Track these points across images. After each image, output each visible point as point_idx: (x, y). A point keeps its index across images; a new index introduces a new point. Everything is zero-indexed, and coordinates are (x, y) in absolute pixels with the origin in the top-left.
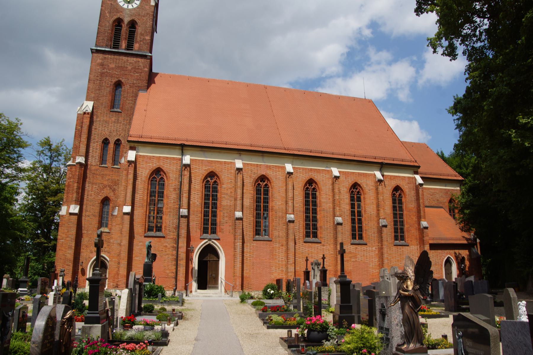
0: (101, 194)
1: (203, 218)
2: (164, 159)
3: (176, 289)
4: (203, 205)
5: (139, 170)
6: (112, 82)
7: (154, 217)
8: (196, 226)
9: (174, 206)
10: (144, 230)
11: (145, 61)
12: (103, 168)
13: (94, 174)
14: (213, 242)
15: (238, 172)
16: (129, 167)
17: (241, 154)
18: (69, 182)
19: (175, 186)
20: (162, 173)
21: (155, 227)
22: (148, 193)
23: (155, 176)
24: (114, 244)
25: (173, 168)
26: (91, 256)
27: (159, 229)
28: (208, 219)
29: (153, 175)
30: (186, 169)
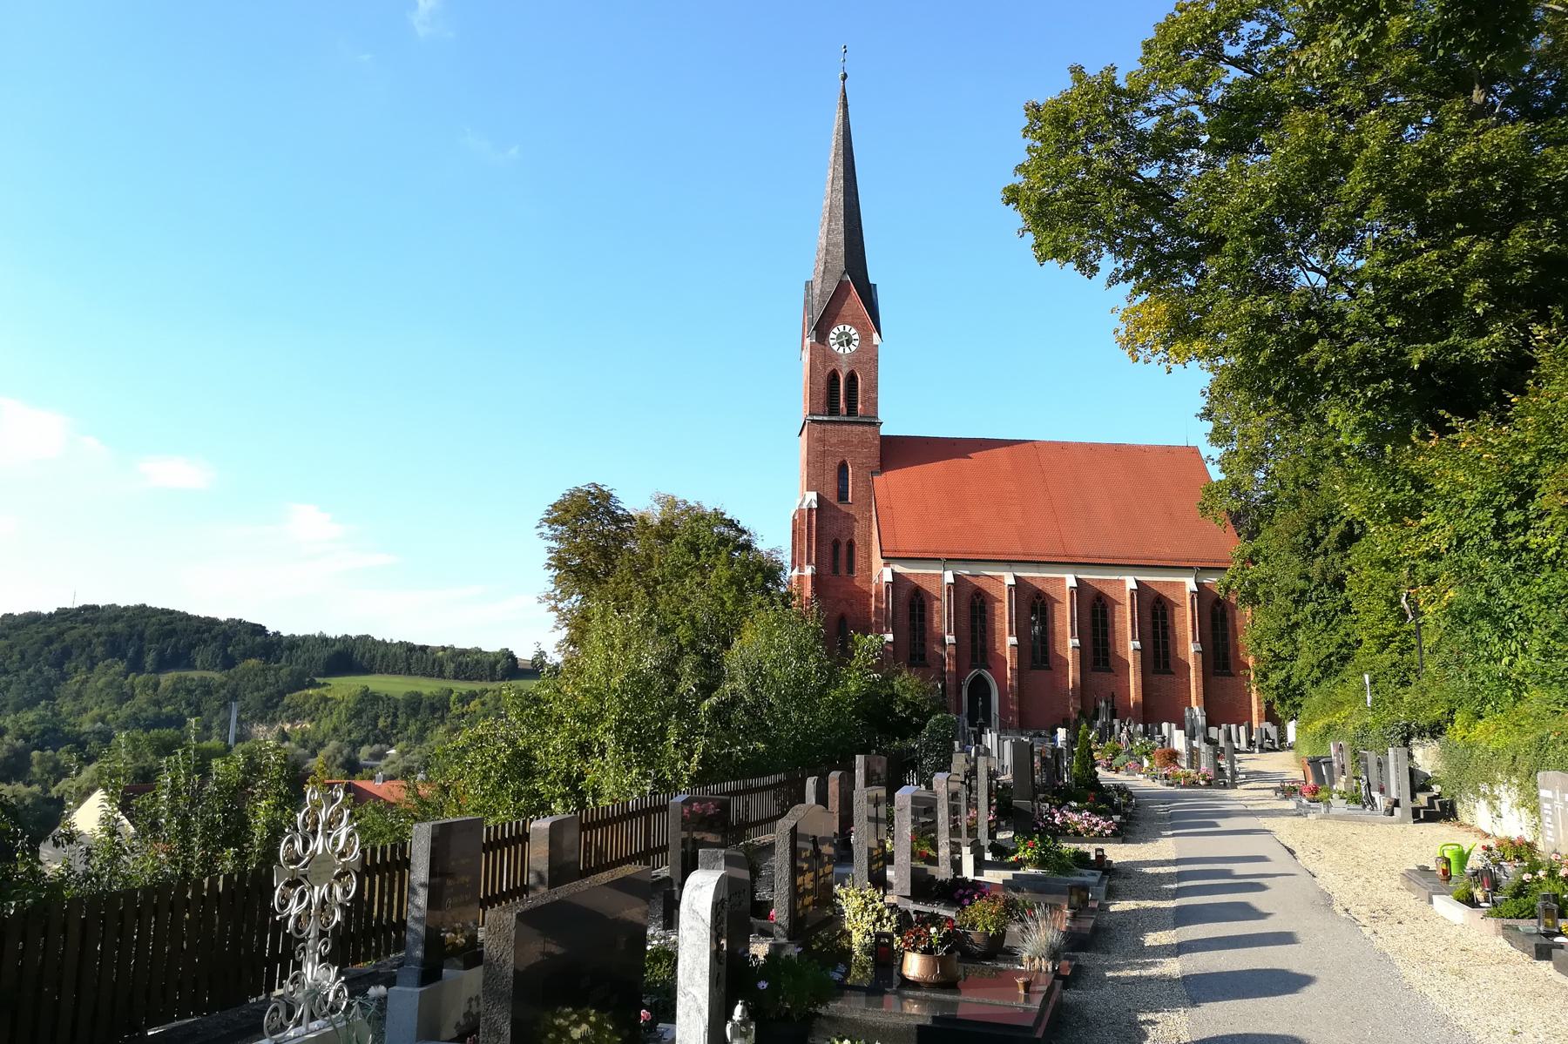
27: (923, 657)
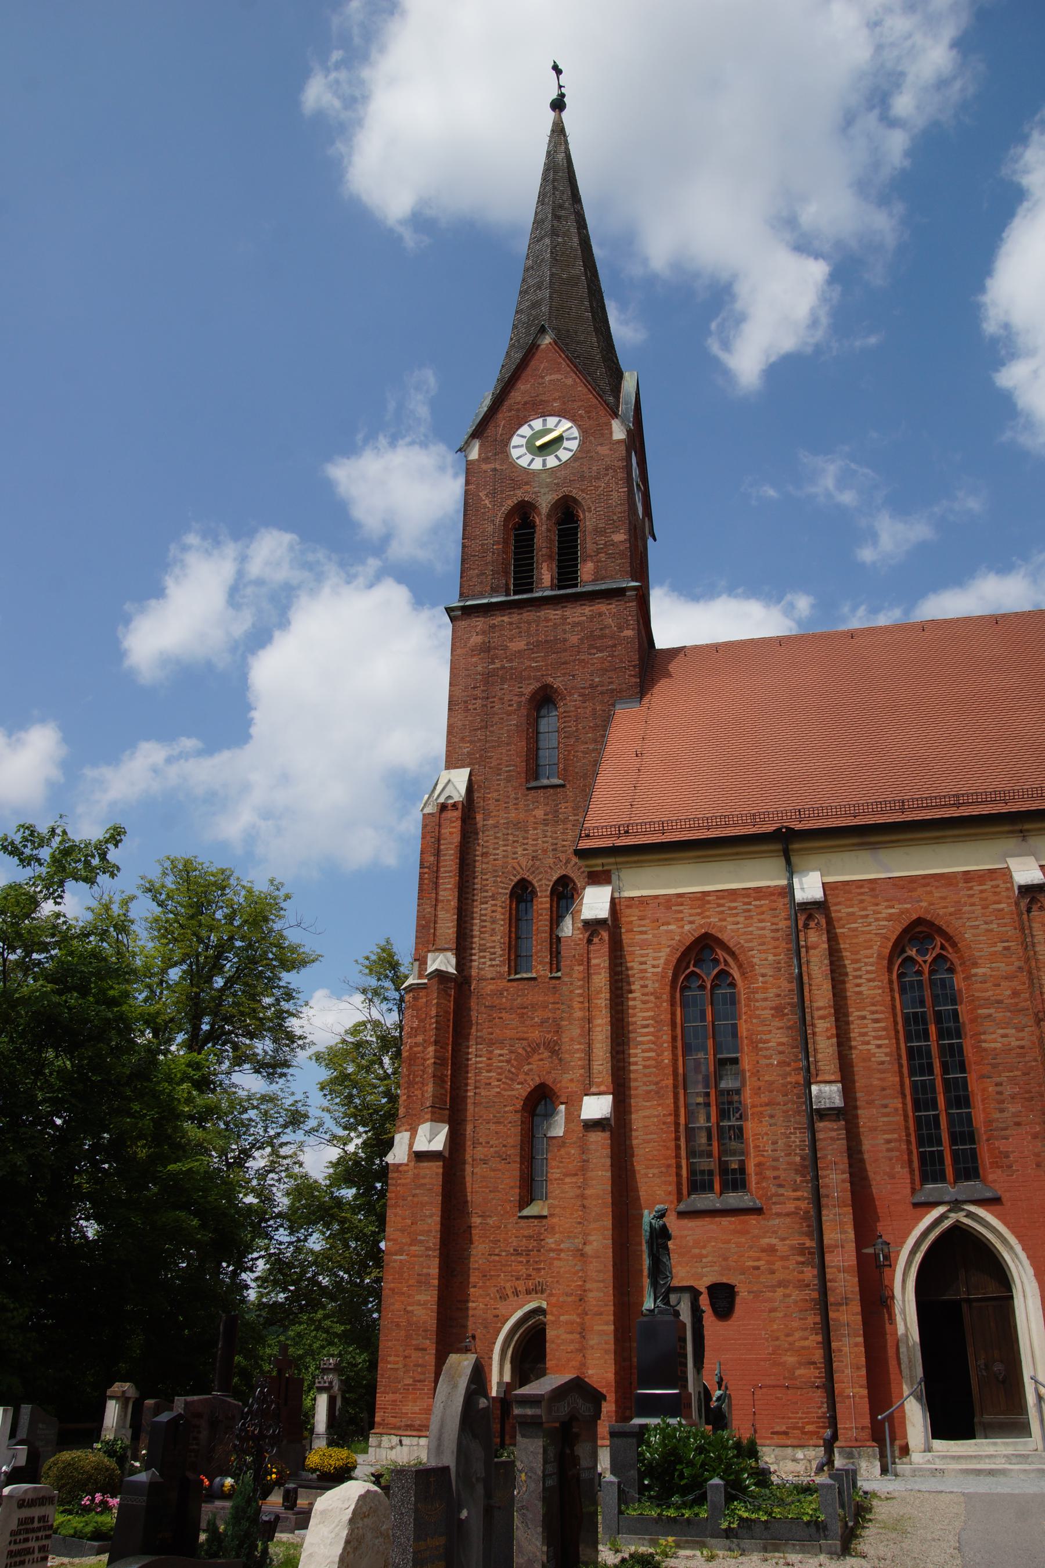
0: (521, 1077)
1: (910, 1114)
2: (723, 898)
3: (835, 1437)
4: (904, 1062)
5: (632, 953)
6: (521, 694)
7: (709, 1130)
8: (889, 1150)
9: (785, 1076)
10: (672, 1188)
11: (621, 608)
12: (521, 985)
13: (492, 1007)
14: (970, 1215)
15: (1031, 902)
16: (592, 948)
17: (1028, 831)
18: (411, 1047)
19: (779, 995)
20: (721, 954)
21: (717, 1171)
22: (674, 1038)
23: (695, 969)
24: (562, 1255)
25: (763, 929)
26: (504, 1312)
27: (736, 1180)
28: (936, 1118)
29: (687, 967)
30: (812, 924)
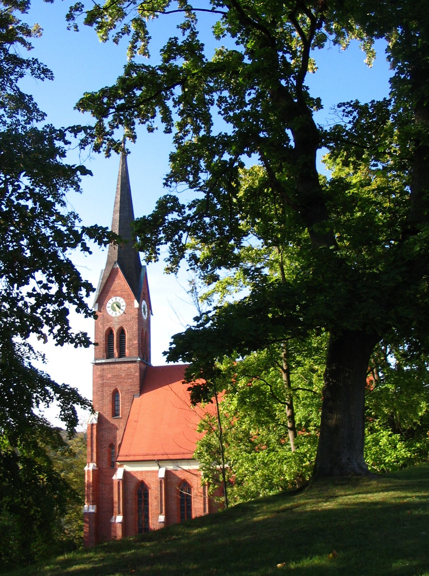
6: (110, 391)
